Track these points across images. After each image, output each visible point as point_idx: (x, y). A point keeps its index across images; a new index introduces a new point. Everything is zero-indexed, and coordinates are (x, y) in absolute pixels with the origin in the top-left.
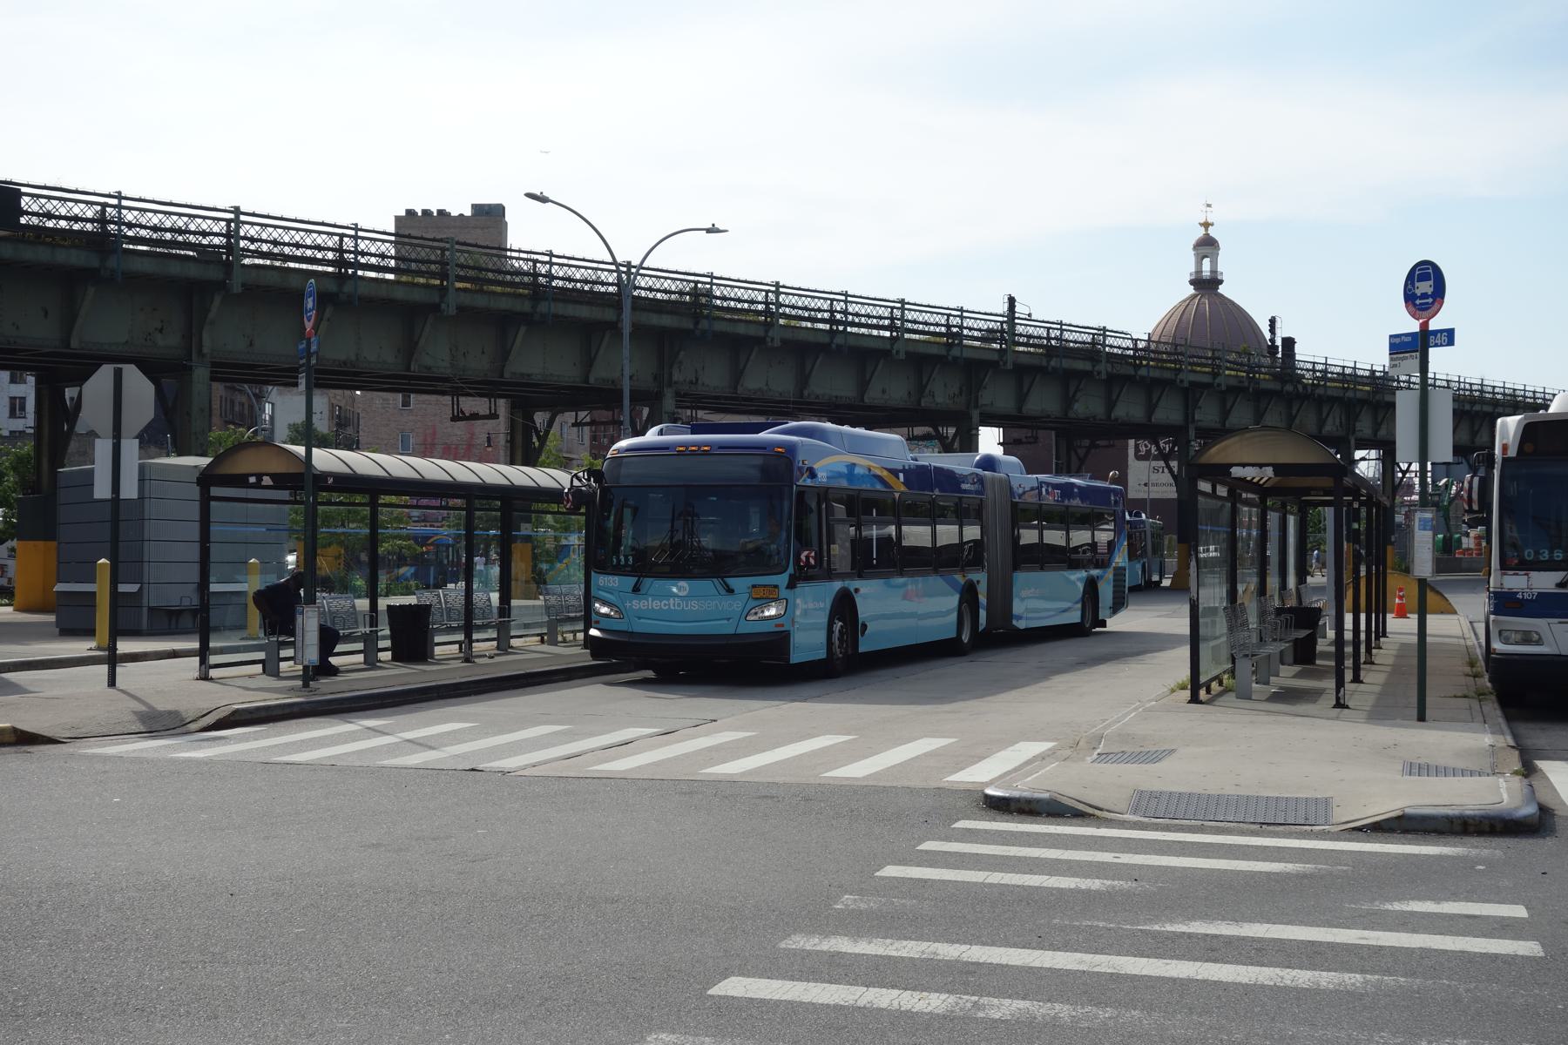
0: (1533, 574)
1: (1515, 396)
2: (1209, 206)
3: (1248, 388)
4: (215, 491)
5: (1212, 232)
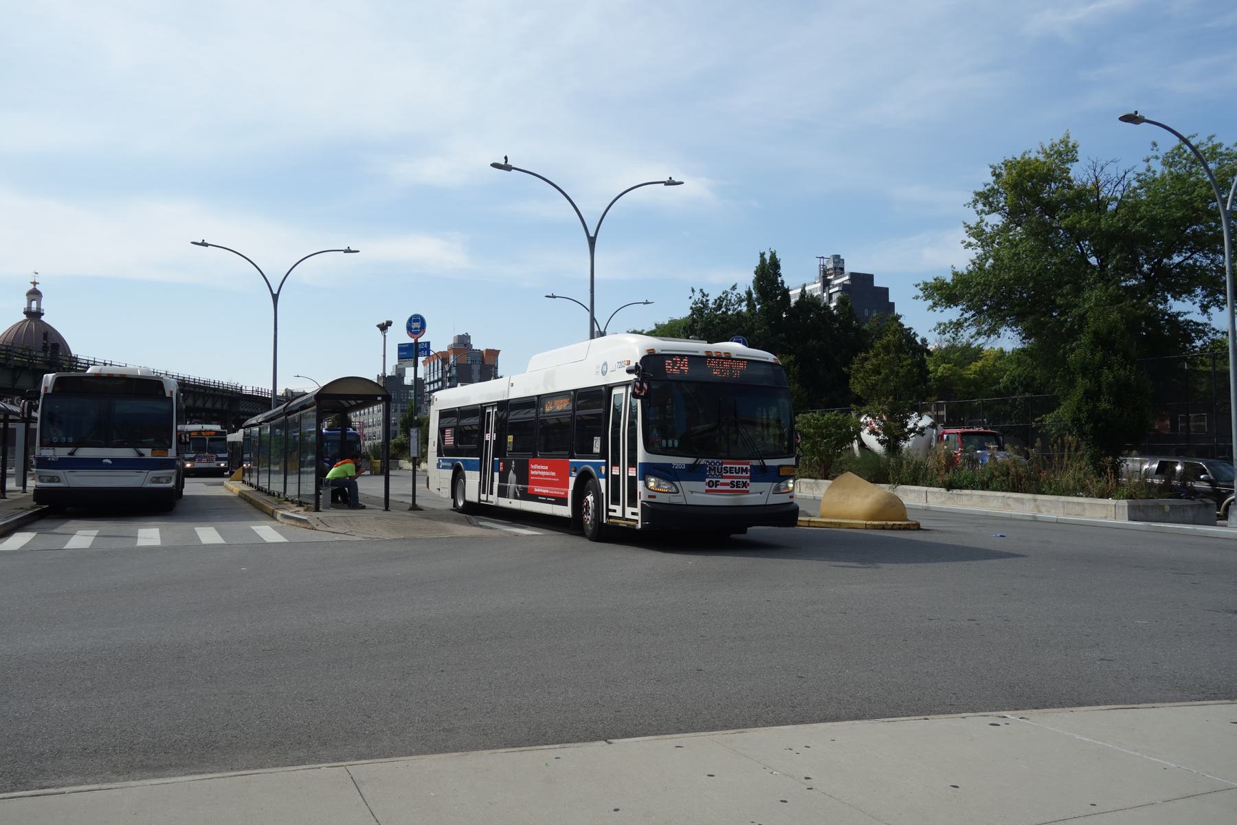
0: (56, 449)
1: (184, 381)
2: (37, 273)
3: (29, 368)
5: (38, 287)
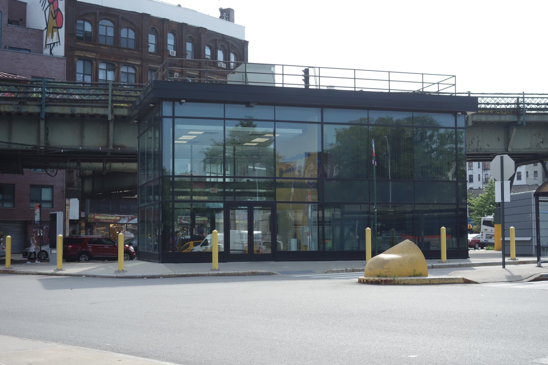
4: (541, 198)
